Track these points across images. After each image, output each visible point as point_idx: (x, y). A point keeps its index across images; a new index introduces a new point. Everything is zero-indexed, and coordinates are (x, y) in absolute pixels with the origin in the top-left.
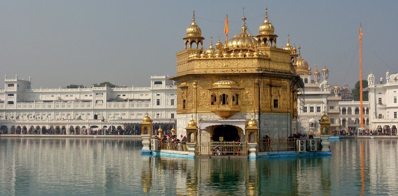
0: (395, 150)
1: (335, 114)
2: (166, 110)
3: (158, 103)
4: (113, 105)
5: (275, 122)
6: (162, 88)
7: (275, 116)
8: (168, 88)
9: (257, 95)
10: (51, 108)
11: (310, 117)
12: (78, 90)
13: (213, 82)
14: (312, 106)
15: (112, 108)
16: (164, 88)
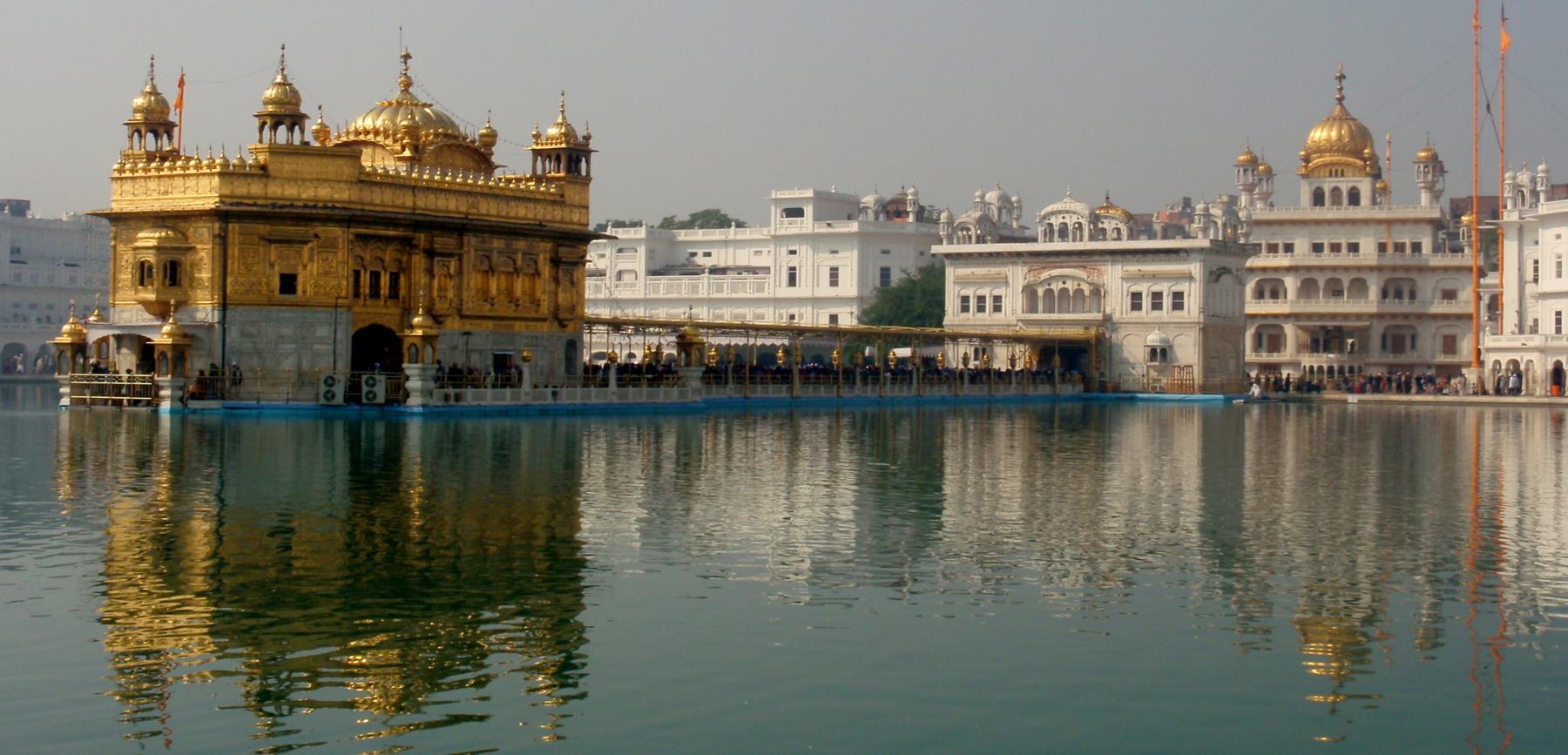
0: (1558, 452)
1: (1459, 317)
2: (816, 301)
3: (792, 281)
4: (665, 286)
5: (286, 331)
6: (804, 231)
7: (288, 315)
8: (822, 229)
9: (218, 264)
10: (700, 296)
11: (1148, 326)
12: (731, 233)
13: (142, 230)
14: (1156, 288)
15: (661, 295)
16: (810, 231)
